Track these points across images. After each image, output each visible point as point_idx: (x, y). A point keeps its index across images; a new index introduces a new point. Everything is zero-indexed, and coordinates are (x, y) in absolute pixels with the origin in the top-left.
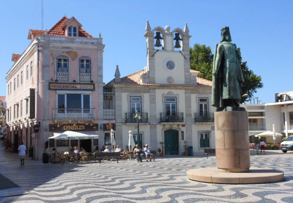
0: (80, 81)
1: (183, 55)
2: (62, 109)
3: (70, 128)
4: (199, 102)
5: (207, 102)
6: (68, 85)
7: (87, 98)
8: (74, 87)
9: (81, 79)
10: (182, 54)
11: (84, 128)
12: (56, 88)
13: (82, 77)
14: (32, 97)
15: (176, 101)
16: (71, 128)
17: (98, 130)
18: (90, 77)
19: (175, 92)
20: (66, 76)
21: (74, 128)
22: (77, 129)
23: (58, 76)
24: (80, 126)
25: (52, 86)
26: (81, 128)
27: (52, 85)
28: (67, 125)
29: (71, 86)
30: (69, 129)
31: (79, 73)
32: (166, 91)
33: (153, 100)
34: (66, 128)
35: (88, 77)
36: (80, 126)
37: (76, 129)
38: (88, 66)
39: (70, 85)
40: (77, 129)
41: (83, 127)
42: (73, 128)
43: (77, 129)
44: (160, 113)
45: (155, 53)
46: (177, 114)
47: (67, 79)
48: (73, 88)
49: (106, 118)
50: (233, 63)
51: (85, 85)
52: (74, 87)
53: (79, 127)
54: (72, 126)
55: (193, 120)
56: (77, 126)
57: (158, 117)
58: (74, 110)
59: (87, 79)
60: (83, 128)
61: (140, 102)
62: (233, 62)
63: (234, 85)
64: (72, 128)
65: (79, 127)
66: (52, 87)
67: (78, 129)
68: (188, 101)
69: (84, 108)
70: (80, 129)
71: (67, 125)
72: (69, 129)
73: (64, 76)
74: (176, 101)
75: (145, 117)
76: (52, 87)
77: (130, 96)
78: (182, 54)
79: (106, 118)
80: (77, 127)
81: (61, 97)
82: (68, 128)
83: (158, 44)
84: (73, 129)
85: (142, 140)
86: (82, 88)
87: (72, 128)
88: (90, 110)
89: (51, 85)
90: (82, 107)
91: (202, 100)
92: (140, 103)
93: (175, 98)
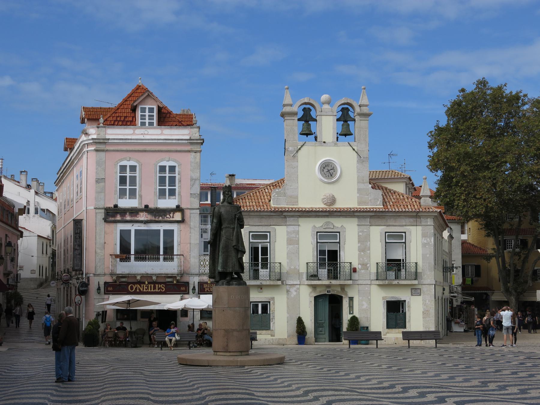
1: (356, 150)
7: (169, 234)
10: (354, 150)
11: (164, 288)
14: (77, 233)
15: (340, 240)
16: (142, 290)
17: (188, 293)
19: (337, 223)
21: (146, 289)
24: (157, 285)
26: (159, 289)
28: (134, 283)
30: (138, 291)
32: (319, 223)
33: (293, 241)
36: (157, 285)
37: (149, 290)
40: (151, 290)
41: (163, 287)
42: (145, 288)
43: (152, 290)
44: (307, 263)
45: (300, 149)
46: (340, 264)
49: (205, 271)
53: (155, 288)
54: (142, 285)
55: (374, 277)
56: (152, 285)
57: (303, 269)
58: (146, 258)
60: (163, 289)
64: (143, 289)
65: (155, 288)
67: (155, 290)
70: (157, 290)
71: (134, 283)
72: (138, 291)
74: (340, 240)
75: (277, 270)
77: (250, 232)
78: (354, 150)
79: (205, 271)
80: (151, 286)
81: (124, 236)
82: (136, 289)
83: (307, 133)
84: (145, 290)
85: (271, 312)
87: (143, 289)
88: (175, 257)
92: (269, 244)
93: (338, 234)
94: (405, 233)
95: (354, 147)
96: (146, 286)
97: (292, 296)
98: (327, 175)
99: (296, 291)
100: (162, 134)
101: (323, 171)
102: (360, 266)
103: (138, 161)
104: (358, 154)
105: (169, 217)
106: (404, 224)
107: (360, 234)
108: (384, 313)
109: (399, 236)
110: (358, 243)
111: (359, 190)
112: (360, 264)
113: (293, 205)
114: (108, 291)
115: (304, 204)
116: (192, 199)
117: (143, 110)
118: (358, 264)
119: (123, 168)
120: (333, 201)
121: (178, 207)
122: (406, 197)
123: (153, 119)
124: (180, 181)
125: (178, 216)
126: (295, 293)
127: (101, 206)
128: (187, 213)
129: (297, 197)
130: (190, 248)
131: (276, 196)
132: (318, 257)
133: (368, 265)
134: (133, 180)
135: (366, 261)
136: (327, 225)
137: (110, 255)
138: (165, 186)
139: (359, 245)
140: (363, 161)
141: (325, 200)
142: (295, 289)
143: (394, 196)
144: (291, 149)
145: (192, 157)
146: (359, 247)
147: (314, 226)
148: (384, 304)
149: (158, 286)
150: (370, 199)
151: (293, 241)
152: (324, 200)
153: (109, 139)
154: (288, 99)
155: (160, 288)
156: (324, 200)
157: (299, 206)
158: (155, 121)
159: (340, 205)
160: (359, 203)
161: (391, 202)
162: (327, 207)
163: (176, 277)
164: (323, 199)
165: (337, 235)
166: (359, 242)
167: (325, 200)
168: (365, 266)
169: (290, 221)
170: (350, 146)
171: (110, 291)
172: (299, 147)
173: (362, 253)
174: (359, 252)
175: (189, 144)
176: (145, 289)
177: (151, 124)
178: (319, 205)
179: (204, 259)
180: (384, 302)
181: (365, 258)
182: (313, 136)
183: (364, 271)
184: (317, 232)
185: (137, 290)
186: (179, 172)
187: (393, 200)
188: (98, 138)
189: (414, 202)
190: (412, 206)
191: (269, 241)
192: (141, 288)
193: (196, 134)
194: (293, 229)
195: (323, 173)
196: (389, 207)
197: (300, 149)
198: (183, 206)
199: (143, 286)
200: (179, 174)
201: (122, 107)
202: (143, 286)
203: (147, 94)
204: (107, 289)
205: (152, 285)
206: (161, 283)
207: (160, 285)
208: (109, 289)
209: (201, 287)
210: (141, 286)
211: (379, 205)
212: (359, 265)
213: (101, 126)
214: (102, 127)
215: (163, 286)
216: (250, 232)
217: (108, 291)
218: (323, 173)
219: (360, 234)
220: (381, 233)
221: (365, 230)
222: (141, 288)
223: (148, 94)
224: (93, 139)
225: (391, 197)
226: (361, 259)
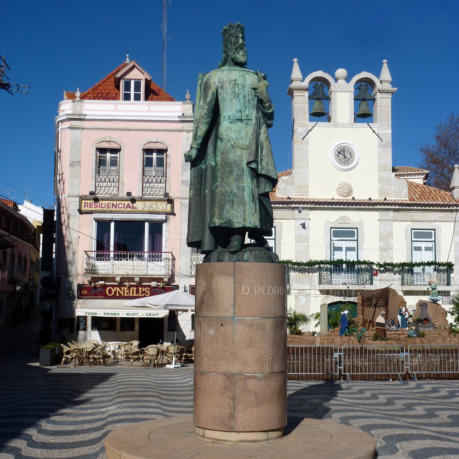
0: (143, 195)
2: (122, 253)
3: (119, 293)
5: (273, 237)
6: (118, 202)
8: (130, 207)
9: (146, 189)
10: (374, 132)
12: (94, 209)
13: (148, 185)
16: (122, 293)
18: (164, 185)
20: (113, 184)
21: (127, 293)
22: (133, 294)
23: (97, 185)
24: (140, 289)
25: (85, 205)
27: (85, 203)
28: (113, 286)
29: (124, 204)
30: (117, 295)
31: (141, 177)
34: (110, 291)
35: (160, 185)
36: (140, 289)
37: (131, 295)
38: (161, 163)
39: (123, 202)
40: (133, 294)
42: (126, 291)
43: (135, 295)
45: (311, 130)
47: (115, 189)
48: (128, 209)
50: (238, 123)
51: (154, 203)
52: (130, 207)
54: (123, 288)
56: (135, 289)
58: (127, 256)
59: (158, 190)
62: (241, 120)
63: (238, 188)
65: (137, 292)
66: (85, 207)
69: (149, 252)
71: (113, 286)
72: (117, 295)
73: (109, 184)
76: (85, 207)
78: (374, 132)
80: (133, 290)
82: (115, 292)
84: (125, 295)
86: (146, 209)
89: (83, 202)
90: (112, 249)
94: (434, 230)
95: (374, 129)
96: (127, 290)
98: (343, 161)
100: (149, 111)
101: (338, 156)
106: (434, 219)
107: (382, 230)
111: (380, 180)
113: (303, 196)
116: (184, 187)
120: (350, 192)
122: (432, 190)
127: (76, 194)
128: (177, 203)
130: (180, 244)
136: (343, 220)
140: (385, 146)
141: (341, 190)
143: (418, 189)
145: (184, 137)
147: (328, 221)
149: (142, 290)
153: (86, 115)
154: (296, 73)
155: (145, 292)
157: (309, 197)
161: (416, 194)
162: (343, 198)
163: (162, 279)
164: (338, 189)
165: (354, 231)
166: (380, 240)
167: (341, 190)
170: (370, 127)
171: (85, 295)
172: (310, 128)
173: (384, 253)
174: (380, 252)
176: (126, 293)
182: (326, 116)
184: (331, 228)
185: (116, 294)
187: (419, 193)
188: (73, 113)
189: (444, 195)
190: (442, 198)
191: (274, 238)
192: (122, 291)
193: (189, 110)
195: (338, 158)
196: (416, 199)
197: (311, 130)
198: (172, 195)
199: (124, 289)
201: (105, 84)
202: (124, 289)
203: (133, 65)
204: (81, 292)
205: (135, 289)
206: (145, 286)
207: (144, 288)
210: (121, 290)
213: (77, 100)
214: (78, 101)
215: (147, 290)
218: (338, 158)
222: (122, 291)
223: (134, 64)
224: (67, 114)
225: (416, 190)
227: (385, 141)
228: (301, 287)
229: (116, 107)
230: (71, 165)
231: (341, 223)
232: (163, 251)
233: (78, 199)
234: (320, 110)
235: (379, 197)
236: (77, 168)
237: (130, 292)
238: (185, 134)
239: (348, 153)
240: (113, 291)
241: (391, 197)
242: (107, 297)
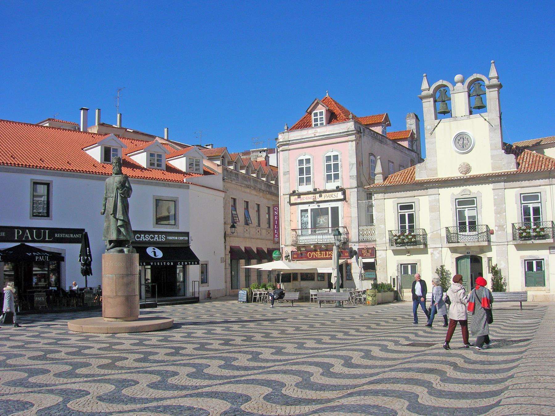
1: (487, 120)
3: (315, 256)
4: (523, 202)
10: (485, 120)
16: (317, 256)
19: (473, 190)
21: (320, 256)
24: (327, 252)
26: (329, 255)
30: (314, 257)
32: (457, 191)
33: (435, 208)
34: (310, 255)
36: (327, 252)
37: (322, 257)
43: (324, 257)
45: (436, 126)
49: (363, 240)
53: (326, 255)
54: (317, 253)
55: (510, 238)
61: (539, 202)
64: (318, 256)
65: (326, 255)
67: (326, 257)
68: (500, 205)
70: (328, 257)
71: (311, 251)
72: (314, 257)
77: (398, 204)
78: (485, 120)
79: (363, 240)
82: (313, 255)
87: (318, 256)
91: (403, 207)
94: (540, 193)
97: (436, 258)
99: (439, 253)
102: (497, 228)
103: (311, 155)
104: (490, 123)
105: (335, 197)
107: (496, 197)
108: (522, 271)
109: (535, 197)
110: (494, 206)
111: (493, 157)
112: (497, 226)
113: (433, 177)
114: (294, 258)
115: (442, 175)
116: (351, 180)
117: (316, 115)
118: (495, 226)
119: (301, 162)
120: (468, 169)
121: (338, 187)
123: (323, 121)
124: (342, 167)
125: (340, 195)
126: (438, 255)
128: (347, 192)
129: (436, 169)
131: (418, 170)
132: (458, 221)
133: (505, 227)
134: (308, 169)
135: (502, 222)
136: (464, 192)
137: (292, 230)
138: (331, 172)
139: (495, 207)
140: (495, 129)
141: (460, 169)
142: (438, 251)
144: (428, 127)
146: (495, 210)
147: (453, 194)
148: (522, 263)
149: (328, 253)
150: (503, 164)
151: (435, 208)
152: (460, 169)
156: (460, 169)
158: (324, 122)
159: (474, 172)
160: (493, 169)
162: (464, 175)
164: (459, 168)
165: (474, 200)
166: (495, 205)
167: (460, 169)
168: (501, 227)
169: (430, 191)
172: (436, 125)
173: (498, 216)
175: (346, 135)
177: (322, 124)
178: (456, 174)
179: (363, 229)
180: (522, 261)
181: (501, 220)
182: (450, 113)
183: (501, 232)
184: (456, 199)
186: (340, 159)
193: (351, 126)
194: (434, 198)
195: (458, 145)
197: (436, 126)
200: (340, 161)
204: (293, 256)
208: (295, 256)
209: (360, 252)
211: (513, 169)
212: (496, 227)
216: (398, 204)
217: (294, 258)
218: (458, 145)
219: (496, 197)
220: (516, 195)
221: (500, 194)
226: (498, 221)
227: (495, 126)
228: (435, 246)
229: (308, 132)
230: (284, 174)
231: (463, 195)
232: (340, 226)
233: (288, 196)
234: (443, 109)
235: (492, 171)
236: (287, 176)
237: (321, 255)
238: (350, 143)
239: (466, 139)
240: (312, 255)
241: (502, 170)
242: (308, 259)
